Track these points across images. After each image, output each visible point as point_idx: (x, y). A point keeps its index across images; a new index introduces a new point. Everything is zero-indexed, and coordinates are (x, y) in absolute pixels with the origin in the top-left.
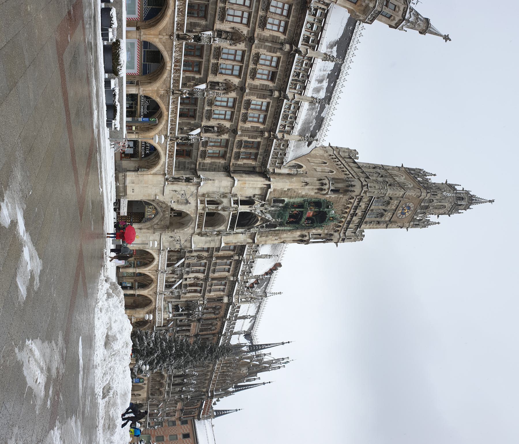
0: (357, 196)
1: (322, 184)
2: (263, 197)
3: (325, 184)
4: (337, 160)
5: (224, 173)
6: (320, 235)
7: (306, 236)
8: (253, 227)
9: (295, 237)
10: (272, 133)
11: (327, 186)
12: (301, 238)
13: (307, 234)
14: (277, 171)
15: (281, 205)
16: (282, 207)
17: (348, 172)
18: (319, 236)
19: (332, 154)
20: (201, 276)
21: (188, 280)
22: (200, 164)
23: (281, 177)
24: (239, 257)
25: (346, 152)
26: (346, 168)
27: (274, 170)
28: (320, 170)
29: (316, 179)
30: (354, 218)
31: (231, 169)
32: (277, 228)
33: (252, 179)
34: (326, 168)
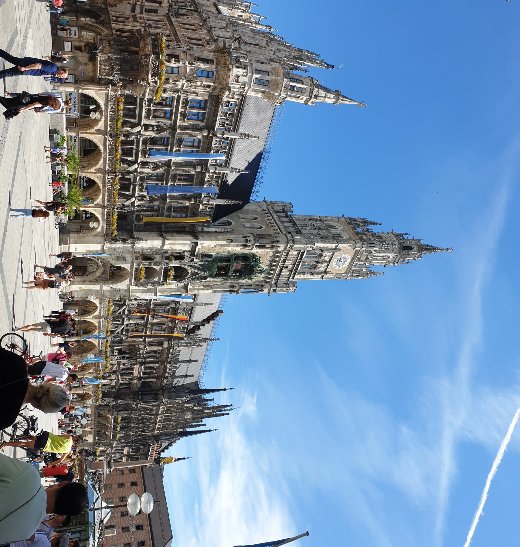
0: (283, 251)
1: (247, 241)
2: (193, 252)
3: (250, 241)
4: (269, 215)
5: (157, 232)
6: (251, 285)
7: (235, 287)
8: (184, 279)
9: (226, 288)
10: (198, 199)
11: (252, 242)
12: (231, 289)
13: (237, 285)
14: (206, 229)
15: (209, 259)
16: (211, 261)
17: (277, 228)
18: (250, 287)
19: (265, 208)
20: (141, 322)
21: (129, 325)
22: (135, 225)
23: (209, 235)
24: (176, 305)
25: (280, 206)
26: (276, 223)
27: (203, 229)
28: (250, 226)
29: (241, 236)
30: (284, 270)
31: (163, 229)
32: (208, 280)
33: (182, 238)
34: (256, 224)
